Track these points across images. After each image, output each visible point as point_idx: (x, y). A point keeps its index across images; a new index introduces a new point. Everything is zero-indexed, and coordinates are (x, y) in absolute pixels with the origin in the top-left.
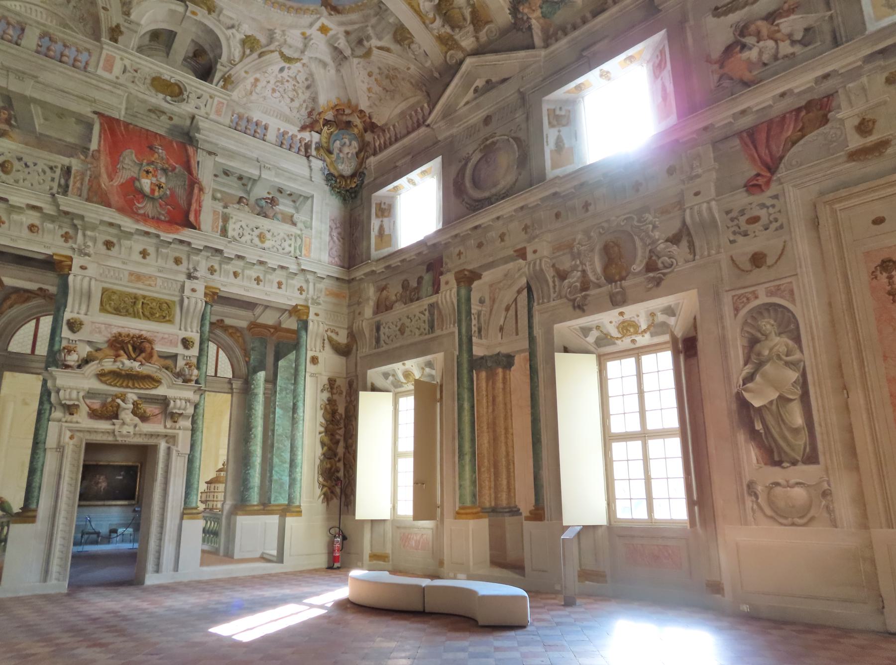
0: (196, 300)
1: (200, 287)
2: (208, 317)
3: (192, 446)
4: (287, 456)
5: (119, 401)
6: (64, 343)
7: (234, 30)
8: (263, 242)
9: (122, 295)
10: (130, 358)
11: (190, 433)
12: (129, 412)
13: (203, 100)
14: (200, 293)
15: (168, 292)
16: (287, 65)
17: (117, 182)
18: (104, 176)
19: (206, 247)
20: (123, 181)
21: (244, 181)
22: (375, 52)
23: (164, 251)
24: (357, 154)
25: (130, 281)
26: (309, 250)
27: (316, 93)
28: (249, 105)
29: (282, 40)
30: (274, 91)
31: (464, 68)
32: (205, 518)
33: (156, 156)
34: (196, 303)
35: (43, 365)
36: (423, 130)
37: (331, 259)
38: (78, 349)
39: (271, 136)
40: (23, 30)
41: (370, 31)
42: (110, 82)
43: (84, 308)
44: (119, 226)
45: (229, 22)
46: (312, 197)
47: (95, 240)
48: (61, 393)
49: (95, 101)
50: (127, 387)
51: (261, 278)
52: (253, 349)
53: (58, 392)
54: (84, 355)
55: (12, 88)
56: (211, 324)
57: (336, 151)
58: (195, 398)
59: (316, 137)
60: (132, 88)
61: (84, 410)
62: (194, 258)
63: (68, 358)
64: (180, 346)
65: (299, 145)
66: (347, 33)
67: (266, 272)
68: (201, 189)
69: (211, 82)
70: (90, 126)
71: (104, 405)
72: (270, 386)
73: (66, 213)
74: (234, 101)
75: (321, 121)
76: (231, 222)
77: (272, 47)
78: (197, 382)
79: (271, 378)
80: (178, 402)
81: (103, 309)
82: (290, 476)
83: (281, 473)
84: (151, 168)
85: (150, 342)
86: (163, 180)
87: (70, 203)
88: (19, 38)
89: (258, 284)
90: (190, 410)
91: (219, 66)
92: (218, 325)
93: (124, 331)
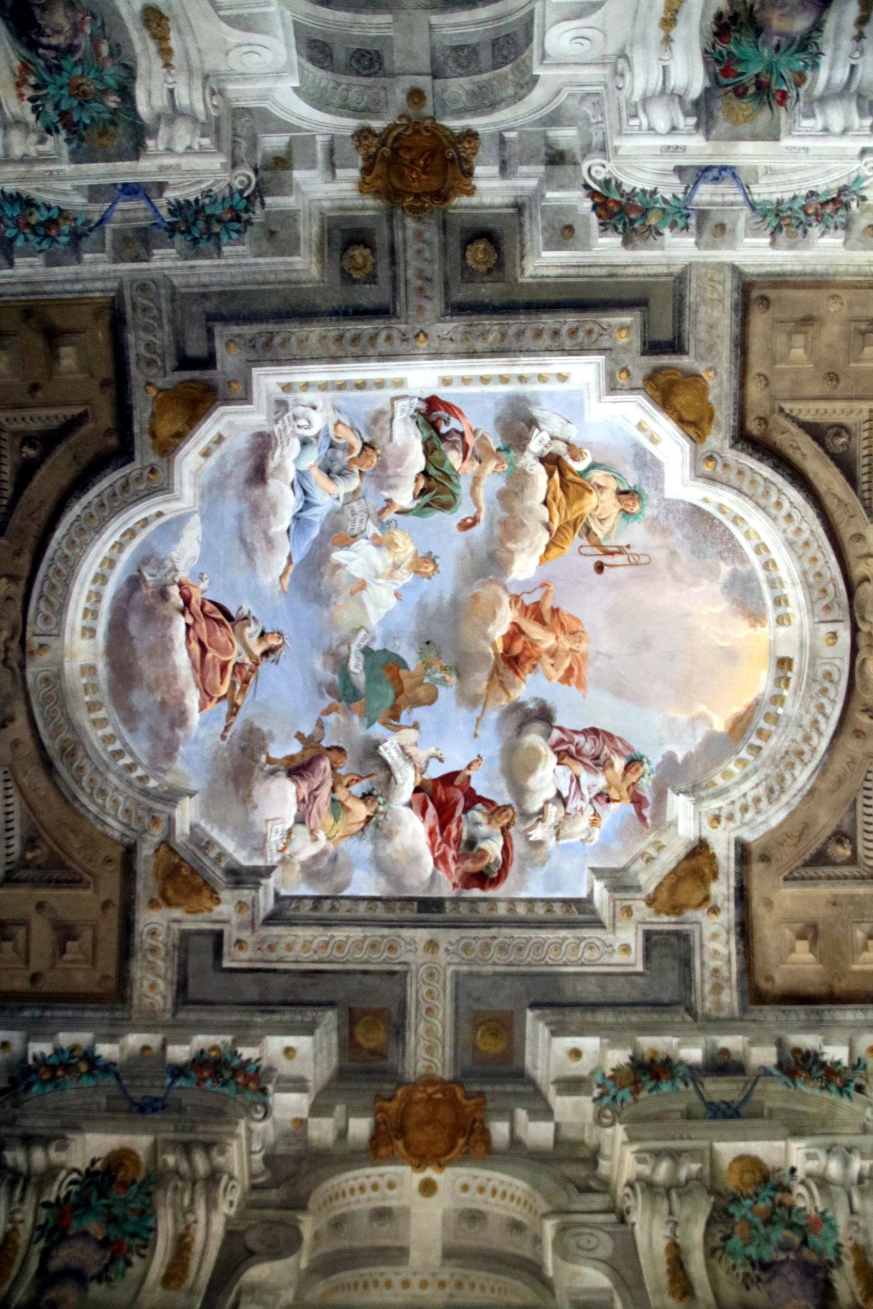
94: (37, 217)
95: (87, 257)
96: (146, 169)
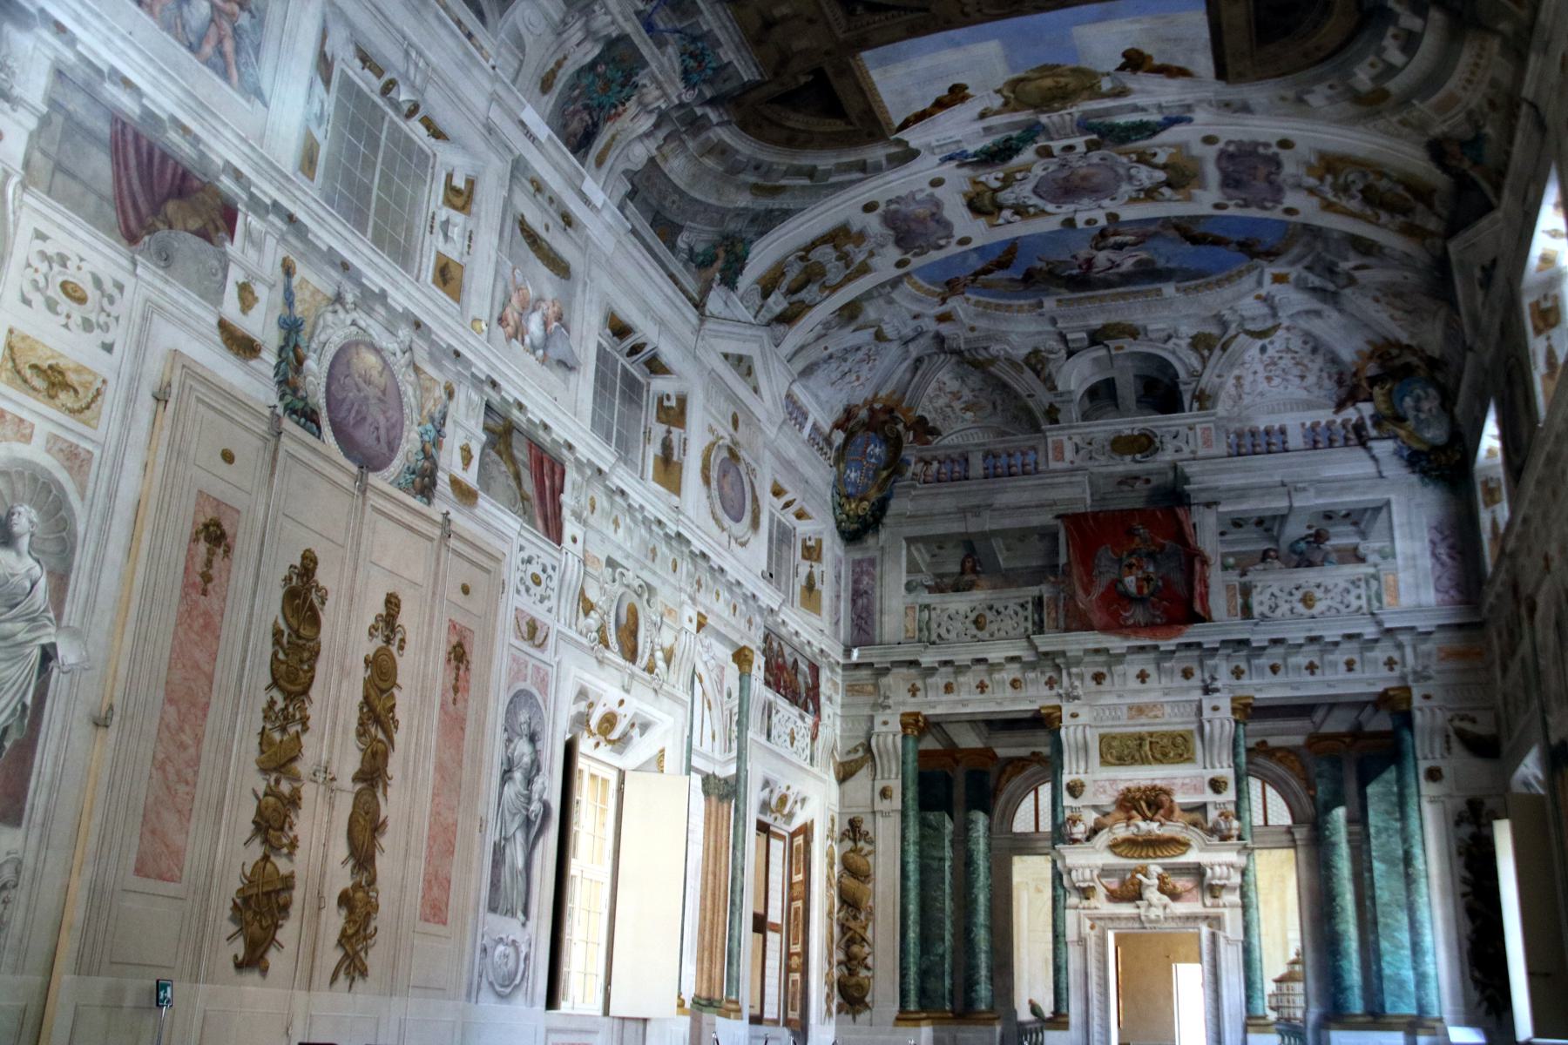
0: (1221, 720)
1: (1225, 703)
3: (1247, 929)
4: (1405, 937)
5: (1140, 876)
6: (1068, 813)
7: (1174, 340)
8: (1310, 607)
10: (1145, 818)
11: (1239, 911)
12: (1154, 889)
13: (1182, 437)
15: (1178, 720)
16: (1266, 341)
17: (1095, 596)
18: (1080, 593)
19: (1223, 642)
20: (1102, 590)
22: (1357, 274)
23: (1167, 665)
24: (1442, 405)
25: (1131, 718)
26: (1396, 596)
27: (1332, 352)
28: (1245, 413)
29: (1236, 318)
30: (1269, 379)
31: (1453, 258)
32: (1280, 1032)
33: (1137, 540)
34: (1222, 726)
35: (1049, 844)
36: (1470, 355)
37: (1440, 596)
38: (1084, 817)
39: (1295, 439)
40: (967, 460)
41: (1329, 257)
43: (1082, 764)
44: (1107, 650)
45: (1164, 334)
46: (1388, 503)
47: (1081, 677)
48: (1074, 874)
49: (1055, 503)
50: (1148, 857)
51: (1317, 662)
52: (1320, 775)
53: (1069, 873)
54: (1091, 823)
55: (972, 529)
57: (1411, 414)
58: (1240, 860)
59: (1367, 409)
60: (1093, 467)
61: (1101, 892)
62: (1210, 662)
63: (1075, 830)
64: (1209, 791)
65: (1343, 432)
66: (1309, 268)
67: (1323, 652)
68: (1205, 562)
69: (1183, 410)
70: (1055, 537)
71: (1123, 883)
72: (1357, 828)
73: (1046, 654)
74: (1222, 418)
75: (1364, 384)
76: (1255, 592)
77: (1232, 332)
78: (1240, 838)
79: (1358, 814)
80: (1217, 869)
81: (1104, 762)
82: (1415, 969)
83: (1396, 964)
85: (1168, 793)
86: (1151, 569)
87: (1045, 643)
88: (966, 471)
89: (1312, 673)
90: (1236, 879)
91: (1182, 387)
92: (1261, 750)
93: (1132, 785)
94: (692, 63)
95: (705, 28)
96: (632, 28)
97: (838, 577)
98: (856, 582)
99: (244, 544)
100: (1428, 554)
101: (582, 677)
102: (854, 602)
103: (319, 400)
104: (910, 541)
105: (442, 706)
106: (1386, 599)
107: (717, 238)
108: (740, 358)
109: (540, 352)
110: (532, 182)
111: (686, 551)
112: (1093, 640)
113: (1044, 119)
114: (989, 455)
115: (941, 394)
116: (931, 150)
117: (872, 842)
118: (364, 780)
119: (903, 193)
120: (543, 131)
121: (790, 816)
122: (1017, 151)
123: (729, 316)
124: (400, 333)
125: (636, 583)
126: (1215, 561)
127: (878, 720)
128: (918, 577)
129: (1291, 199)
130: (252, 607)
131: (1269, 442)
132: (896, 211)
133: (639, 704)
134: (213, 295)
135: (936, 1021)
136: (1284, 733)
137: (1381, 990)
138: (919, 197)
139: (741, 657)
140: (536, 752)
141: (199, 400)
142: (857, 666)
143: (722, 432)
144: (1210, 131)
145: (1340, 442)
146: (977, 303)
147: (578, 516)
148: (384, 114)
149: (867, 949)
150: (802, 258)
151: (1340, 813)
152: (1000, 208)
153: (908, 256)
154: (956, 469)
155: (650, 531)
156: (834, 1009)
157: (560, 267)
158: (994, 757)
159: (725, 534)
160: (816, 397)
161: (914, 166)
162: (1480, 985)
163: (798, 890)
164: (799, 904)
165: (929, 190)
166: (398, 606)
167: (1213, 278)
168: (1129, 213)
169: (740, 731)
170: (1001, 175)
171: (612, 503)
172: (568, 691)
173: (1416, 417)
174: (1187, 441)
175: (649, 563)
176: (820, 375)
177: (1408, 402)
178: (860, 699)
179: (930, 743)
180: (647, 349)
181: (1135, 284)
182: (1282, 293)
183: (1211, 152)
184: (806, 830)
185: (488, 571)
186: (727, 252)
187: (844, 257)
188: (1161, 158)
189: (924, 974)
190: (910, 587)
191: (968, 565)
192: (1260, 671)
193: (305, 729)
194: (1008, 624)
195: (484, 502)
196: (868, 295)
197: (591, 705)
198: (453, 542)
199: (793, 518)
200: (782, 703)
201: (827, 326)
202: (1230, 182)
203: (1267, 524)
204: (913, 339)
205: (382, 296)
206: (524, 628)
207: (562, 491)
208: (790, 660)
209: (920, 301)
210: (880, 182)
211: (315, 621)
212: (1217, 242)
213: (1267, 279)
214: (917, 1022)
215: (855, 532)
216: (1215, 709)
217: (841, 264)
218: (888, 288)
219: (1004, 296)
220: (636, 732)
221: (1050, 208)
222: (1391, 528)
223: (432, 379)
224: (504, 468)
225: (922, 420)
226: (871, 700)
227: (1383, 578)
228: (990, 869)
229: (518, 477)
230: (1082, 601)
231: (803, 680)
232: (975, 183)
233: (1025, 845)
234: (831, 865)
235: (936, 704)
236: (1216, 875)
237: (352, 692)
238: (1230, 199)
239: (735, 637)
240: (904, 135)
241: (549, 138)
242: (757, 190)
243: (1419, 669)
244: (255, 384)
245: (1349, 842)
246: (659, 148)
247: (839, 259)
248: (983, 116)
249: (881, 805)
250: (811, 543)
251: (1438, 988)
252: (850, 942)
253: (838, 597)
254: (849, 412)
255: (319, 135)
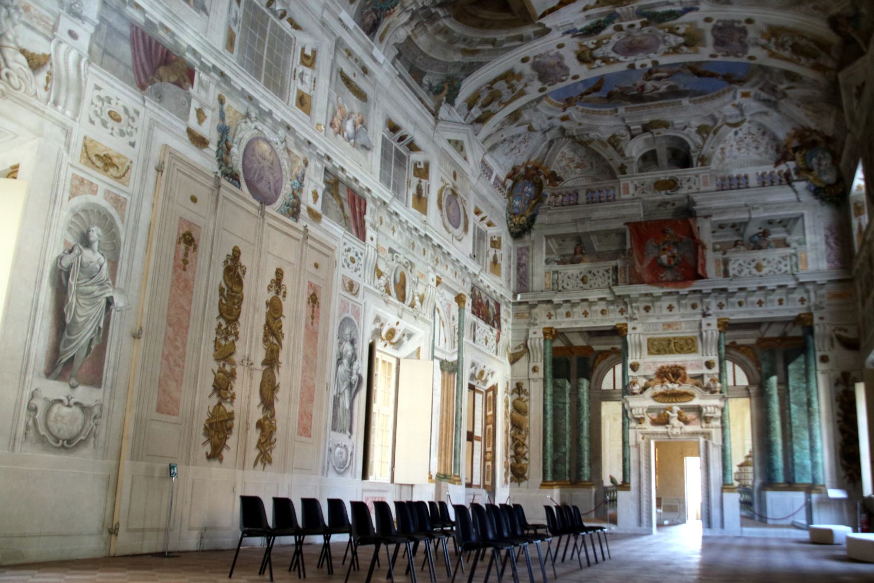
0: (712, 330)
1: (714, 321)
2: (723, 342)
3: (724, 439)
4: (806, 443)
5: (668, 412)
6: (630, 380)
7: (688, 129)
9: (660, 340)
10: (671, 382)
11: (720, 430)
13: (692, 181)
14: (714, 326)
16: (738, 129)
17: (645, 265)
18: (637, 264)
19: (714, 290)
21: (737, 227)
22: (788, 92)
23: (683, 302)
25: (664, 330)
30: (739, 149)
32: (740, 492)
34: (712, 334)
35: (620, 395)
39: (753, 181)
40: (577, 194)
41: (772, 82)
42: (629, 200)
43: (638, 354)
44: (651, 294)
45: (682, 126)
46: (802, 215)
47: (638, 308)
48: (633, 411)
49: (624, 217)
51: (763, 299)
52: (764, 360)
53: (631, 410)
54: (643, 385)
55: (580, 231)
56: (726, 347)
57: (816, 167)
59: (792, 165)
60: (645, 197)
61: (648, 420)
62: (706, 300)
63: (634, 388)
66: (761, 89)
67: (766, 295)
68: (704, 247)
69: (692, 166)
70: (624, 234)
71: (659, 416)
72: (782, 387)
73: (619, 296)
75: (791, 151)
76: (730, 263)
77: (719, 124)
78: (721, 392)
80: (709, 408)
81: (650, 353)
83: (802, 457)
84: (666, 247)
85: (683, 369)
86: (675, 251)
87: (620, 290)
89: (761, 306)
91: (692, 154)
92: (732, 346)
93: (664, 365)
97: (510, 257)
98: (519, 259)
99: (204, 245)
100: (824, 242)
101: (378, 310)
102: (518, 269)
103: (239, 168)
104: (548, 237)
105: (306, 326)
106: (800, 267)
107: (444, 78)
108: (457, 142)
109: (352, 141)
110: (346, 50)
111: (430, 244)
112: (643, 289)
113: (618, 10)
114: (589, 191)
115: (563, 159)
116: (558, 28)
117: (528, 395)
118: (267, 364)
119: (542, 52)
120: (351, 24)
121: (486, 381)
122: (604, 28)
123: (451, 119)
124: (280, 133)
125: (404, 261)
126: (709, 246)
127: (531, 332)
128: (552, 256)
129: (753, 51)
130: (208, 277)
131: (739, 183)
132: (539, 62)
133: (406, 324)
134: (185, 116)
135: (562, 486)
136: (745, 337)
137: (793, 471)
138: (551, 54)
139: (460, 299)
140: (354, 349)
141: (178, 170)
142: (520, 303)
143: (448, 181)
144: (708, 15)
145: (777, 182)
146: (582, 111)
147: (373, 227)
148: (268, 18)
149: (525, 450)
150: (489, 88)
151: (774, 379)
152: (595, 59)
153: (546, 86)
154: (571, 199)
155: (411, 233)
156: (509, 480)
157: (361, 95)
158: (592, 350)
159: (450, 235)
160: (497, 161)
161: (548, 37)
162: (846, 468)
163: (490, 419)
164: (490, 426)
165: (556, 50)
166: (282, 274)
167: (709, 95)
168: (664, 61)
169: (459, 338)
170: (595, 41)
171: (391, 219)
172: (370, 318)
173: (819, 169)
174: (695, 183)
175: (411, 250)
176: (499, 150)
177: (814, 161)
178: (522, 321)
179: (558, 343)
180: (408, 138)
181: (667, 98)
182: (746, 102)
183: (709, 26)
184: (494, 389)
185: (328, 256)
186: (449, 85)
187: (511, 87)
188: (682, 30)
189: (555, 462)
190: (547, 262)
191: (578, 250)
192: (733, 304)
193: (237, 338)
194: (599, 281)
195: (326, 222)
196: (524, 107)
197: (382, 325)
198: (309, 241)
199: (486, 226)
200: (481, 323)
201: (503, 124)
202: (719, 43)
203: (738, 227)
204: (549, 130)
205: (270, 113)
206: (347, 285)
207: (365, 213)
208: (485, 300)
209: (551, 109)
210: (530, 46)
211: (240, 283)
212: (712, 75)
213: (739, 95)
214: (551, 486)
215: (518, 233)
216: (709, 325)
217: (510, 91)
218: (535, 103)
219: (596, 107)
220: (405, 338)
221: (621, 58)
222: (804, 229)
223: (297, 156)
224: (335, 202)
225: (553, 173)
226: (527, 321)
227: (799, 255)
228: (590, 409)
229: (342, 207)
230: (638, 268)
231: (492, 311)
232: (581, 46)
233: (608, 396)
234: (507, 407)
235: (562, 323)
236: (708, 411)
237: (260, 320)
238: (719, 51)
239: (456, 289)
240: (543, 21)
241: (355, 27)
242: (465, 52)
243: (818, 303)
244: (205, 161)
245: (779, 394)
246: (412, 31)
247: (509, 88)
248: (585, 9)
249: (533, 375)
250: (495, 239)
251: (823, 469)
252: (517, 446)
253: (510, 267)
254: (515, 170)
255: (235, 29)
